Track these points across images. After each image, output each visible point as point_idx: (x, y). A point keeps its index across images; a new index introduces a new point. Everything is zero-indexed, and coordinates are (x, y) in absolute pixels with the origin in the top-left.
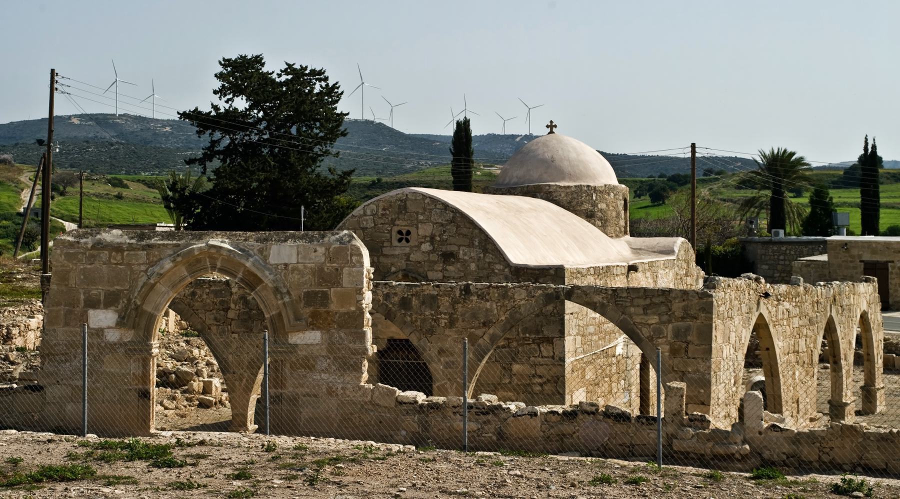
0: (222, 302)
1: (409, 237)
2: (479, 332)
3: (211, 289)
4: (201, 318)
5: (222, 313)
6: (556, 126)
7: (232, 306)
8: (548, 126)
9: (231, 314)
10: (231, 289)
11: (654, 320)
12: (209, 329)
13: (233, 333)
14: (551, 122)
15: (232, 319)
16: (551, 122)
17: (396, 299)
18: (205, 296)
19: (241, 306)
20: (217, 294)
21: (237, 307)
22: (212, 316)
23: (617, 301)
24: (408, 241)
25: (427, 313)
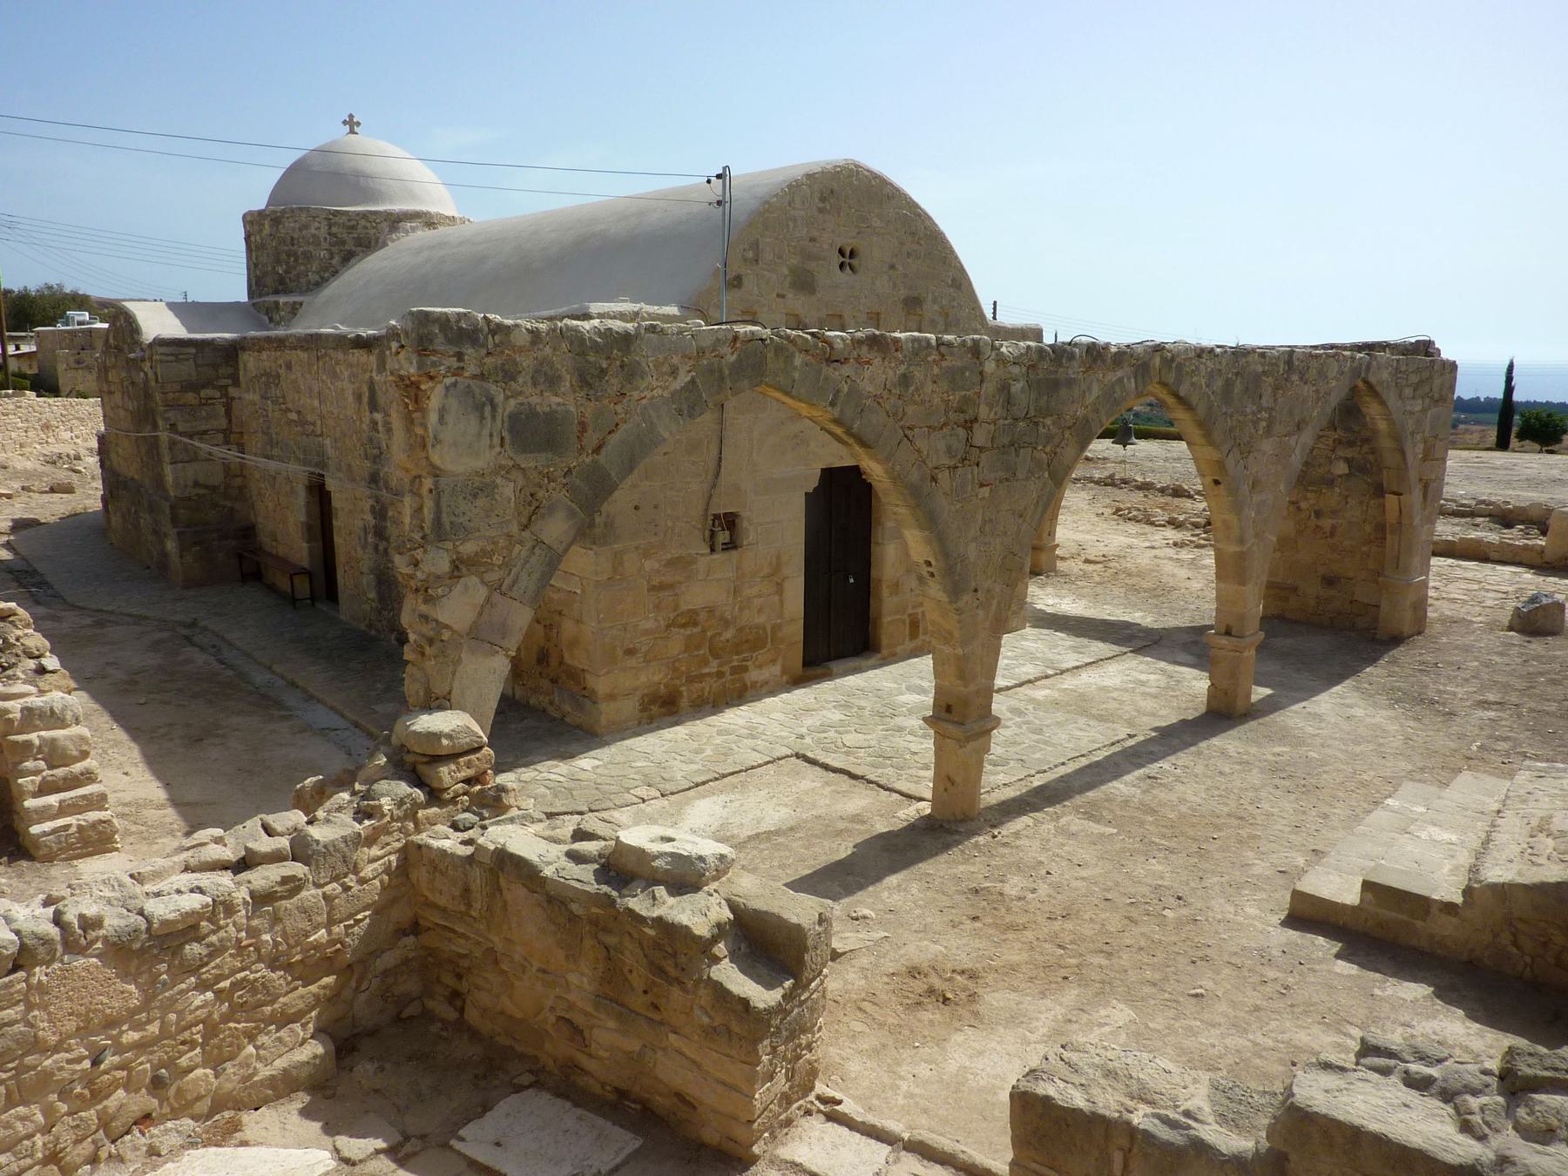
0: (966, 400)
1: (855, 262)
2: (1292, 441)
3: (944, 364)
4: (919, 451)
5: (961, 432)
6: (358, 124)
7: (983, 412)
8: (345, 122)
9: (980, 436)
10: (981, 364)
11: (1417, 406)
12: (934, 479)
13: (982, 485)
14: (351, 116)
15: (981, 449)
16: (351, 116)
17: (1219, 383)
18: (929, 387)
19: (998, 409)
20: (953, 377)
21: (992, 415)
22: (942, 445)
23: (1398, 378)
24: (852, 268)
25: (1248, 410)
